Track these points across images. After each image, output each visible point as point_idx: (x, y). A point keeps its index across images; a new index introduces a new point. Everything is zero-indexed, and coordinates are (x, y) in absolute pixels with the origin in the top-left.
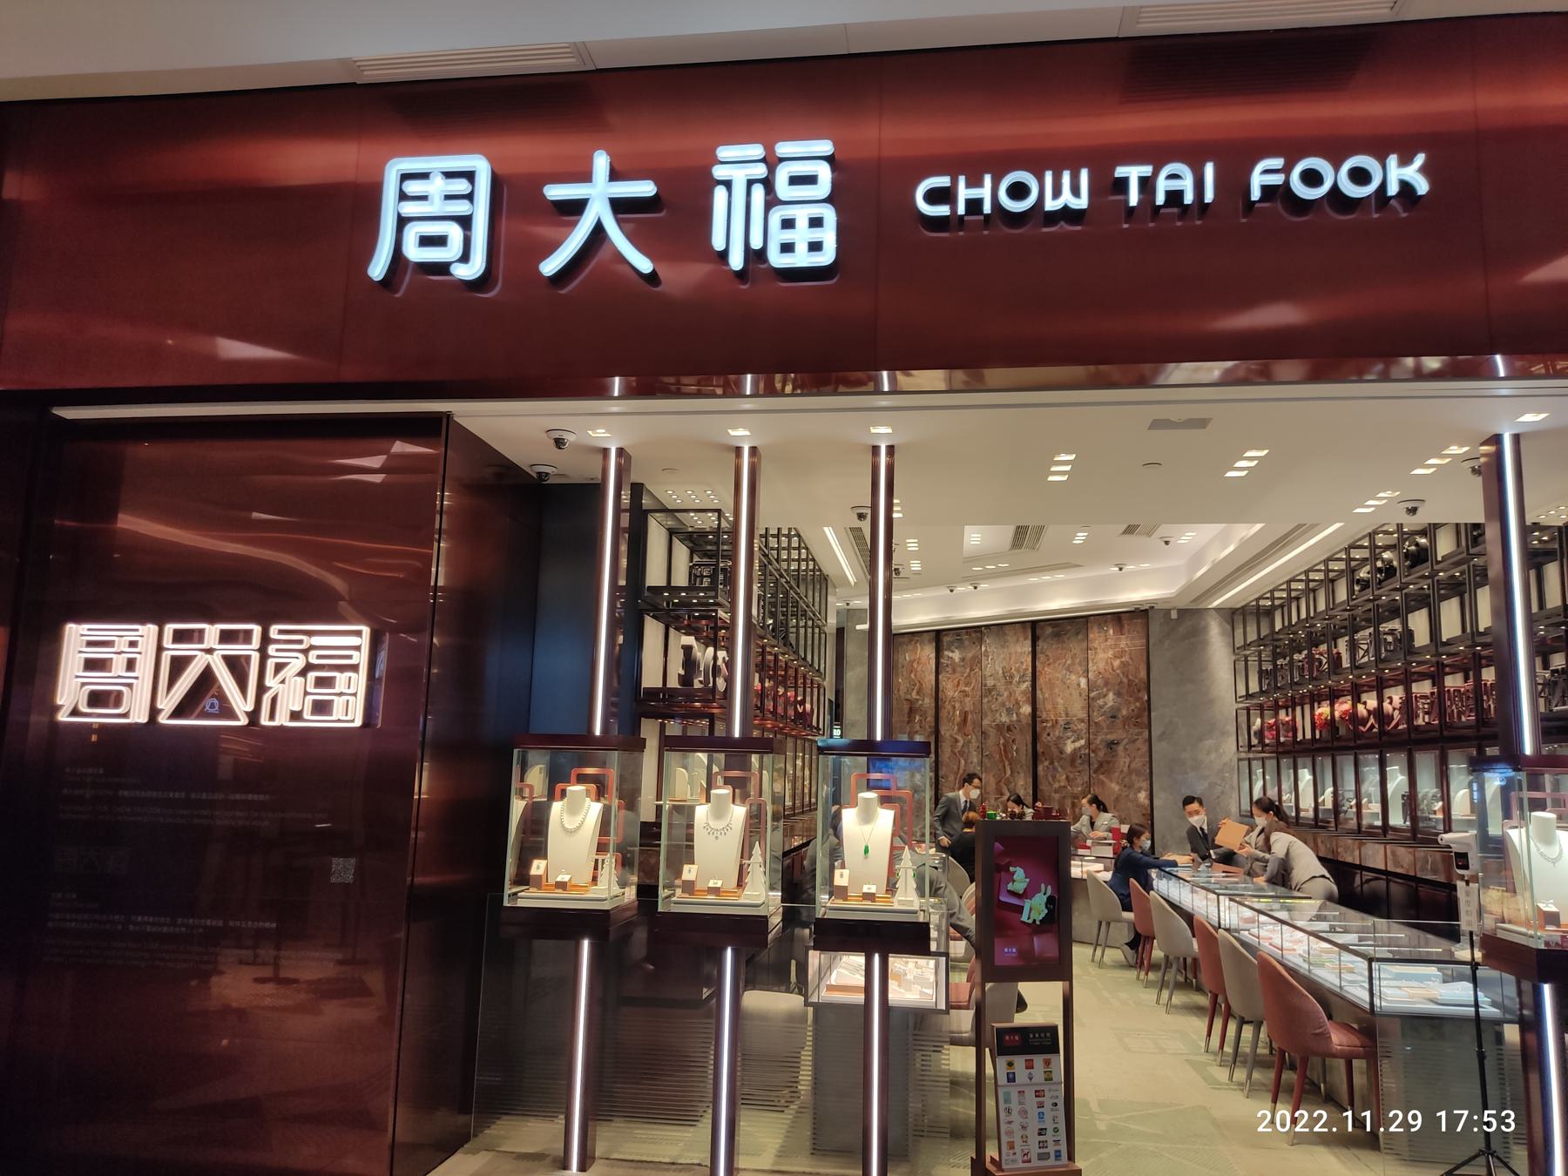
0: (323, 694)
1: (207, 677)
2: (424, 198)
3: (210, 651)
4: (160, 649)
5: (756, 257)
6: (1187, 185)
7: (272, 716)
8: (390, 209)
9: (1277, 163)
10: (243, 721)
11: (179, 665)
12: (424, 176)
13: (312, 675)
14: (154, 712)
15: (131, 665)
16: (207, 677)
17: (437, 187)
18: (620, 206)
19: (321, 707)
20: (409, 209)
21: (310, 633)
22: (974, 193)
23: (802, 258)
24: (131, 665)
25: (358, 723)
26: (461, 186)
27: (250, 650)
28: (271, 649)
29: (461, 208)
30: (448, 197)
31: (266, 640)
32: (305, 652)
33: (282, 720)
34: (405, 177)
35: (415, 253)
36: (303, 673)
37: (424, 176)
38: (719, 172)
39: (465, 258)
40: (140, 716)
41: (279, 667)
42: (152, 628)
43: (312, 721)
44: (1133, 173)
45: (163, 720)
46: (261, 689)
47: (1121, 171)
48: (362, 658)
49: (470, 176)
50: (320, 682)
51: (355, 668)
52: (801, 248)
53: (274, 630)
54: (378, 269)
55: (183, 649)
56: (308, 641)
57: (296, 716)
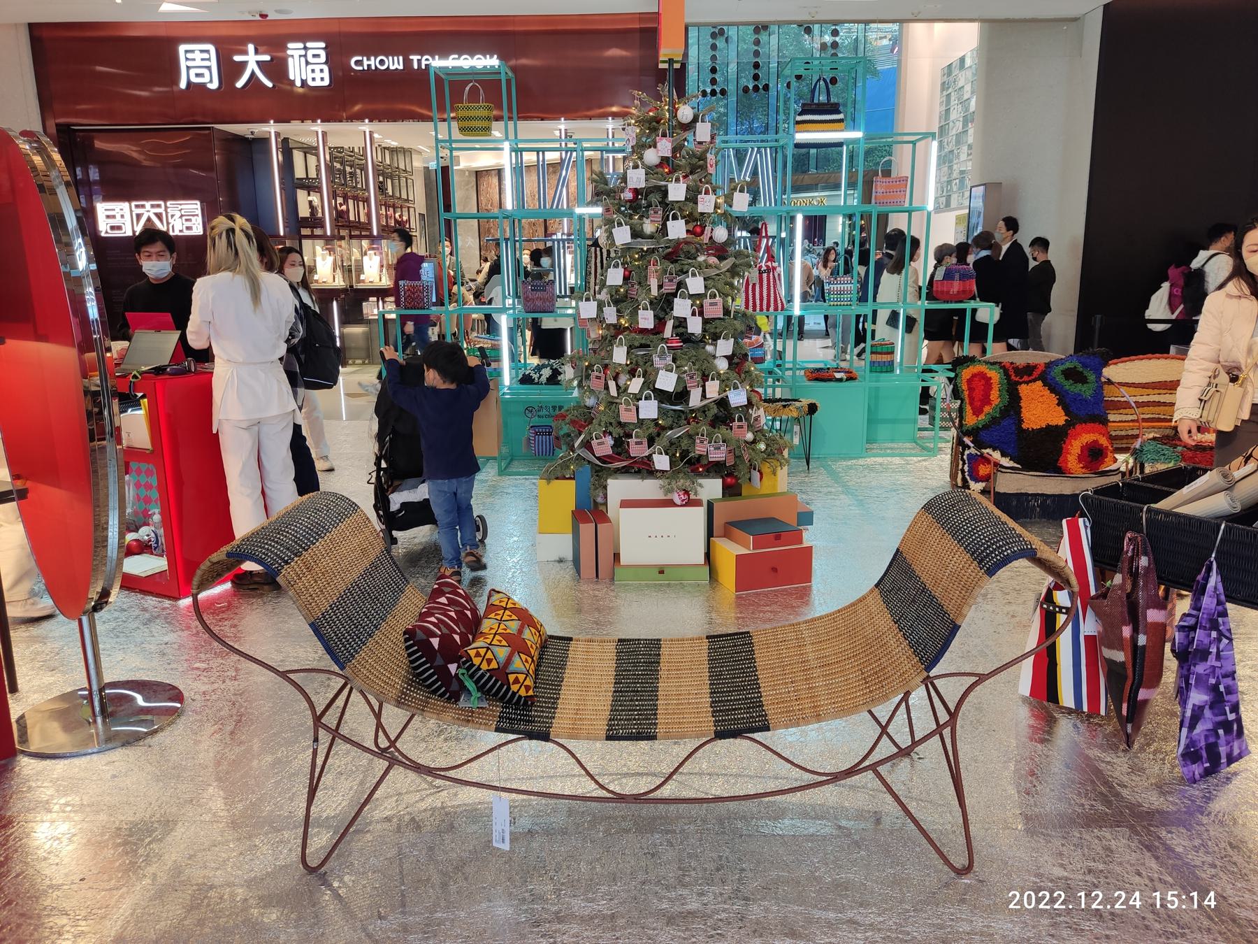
0: (188, 224)
3: (148, 211)
4: (131, 211)
5: (304, 83)
11: (139, 216)
13: (184, 218)
15: (122, 216)
19: (188, 228)
21: (181, 204)
23: (318, 83)
24: (122, 216)
25: (202, 233)
28: (169, 210)
31: (166, 208)
32: (180, 210)
33: (177, 233)
35: (194, 80)
36: (182, 216)
39: (211, 81)
41: (172, 216)
46: (168, 223)
48: (199, 212)
50: (187, 220)
51: (197, 215)
52: (318, 79)
54: (183, 85)
55: (140, 211)
56: (180, 207)
57: (181, 231)
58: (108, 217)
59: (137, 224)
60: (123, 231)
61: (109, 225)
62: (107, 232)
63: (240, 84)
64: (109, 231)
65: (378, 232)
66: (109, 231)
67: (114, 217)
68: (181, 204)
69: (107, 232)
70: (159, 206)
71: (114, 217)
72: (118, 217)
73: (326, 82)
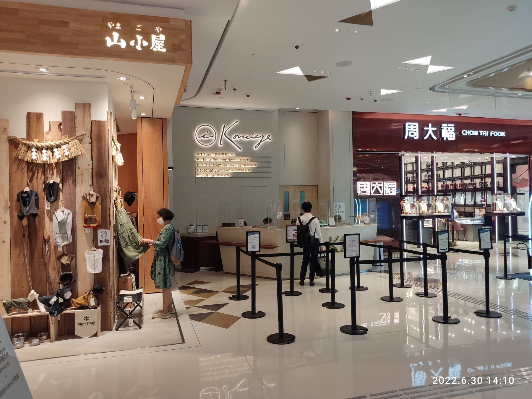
0: (391, 191)
1: (377, 189)
2: (410, 128)
4: (370, 185)
5: (447, 138)
6: (485, 134)
7: (385, 194)
8: (407, 130)
9: (493, 132)
10: (382, 194)
11: (373, 187)
12: (410, 125)
13: (389, 188)
14: (371, 194)
15: (367, 187)
16: (377, 189)
17: (412, 127)
18: (432, 130)
19: (391, 192)
20: (409, 130)
21: (389, 183)
22: (467, 133)
24: (367, 187)
26: (415, 127)
27: (381, 185)
28: (384, 185)
29: (415, 130)
30: (414, 128)
31: (383, 184)
33: (387, 194)
34: (409, 125)
35: (410, 135)
36: (389, 187)
37: (410, 125)
38: (442, 127)
39: (416, 136)
40: (369, 194)
41: (385, 187)
42: (369, 182)
43: (390, 194)
44: (481, 132)
45: (372, 195)
46: (384, 190)
47: (480, 132)
48: (395, 186)
49: (415, 125)
50: (391, 189)
51: (394, 187)
53: (384, 183)
54: (406, 137)
55: (373, 185)
56: (389, 184)
57: (388, 193)
58: (361, 187)
59: (372, 190)
60: (366, 194)
61: (361, 191)
62: (360, 194)
63: (425, 138)
64: (390, 193)
65: (405, 194)
66: (361, 193)
67: (363, 187)
68: (389, 183)
69: (360, 194)
70: (380, 183)
71: (363, 187)
72: (365, 187)
73: (454, 139)
